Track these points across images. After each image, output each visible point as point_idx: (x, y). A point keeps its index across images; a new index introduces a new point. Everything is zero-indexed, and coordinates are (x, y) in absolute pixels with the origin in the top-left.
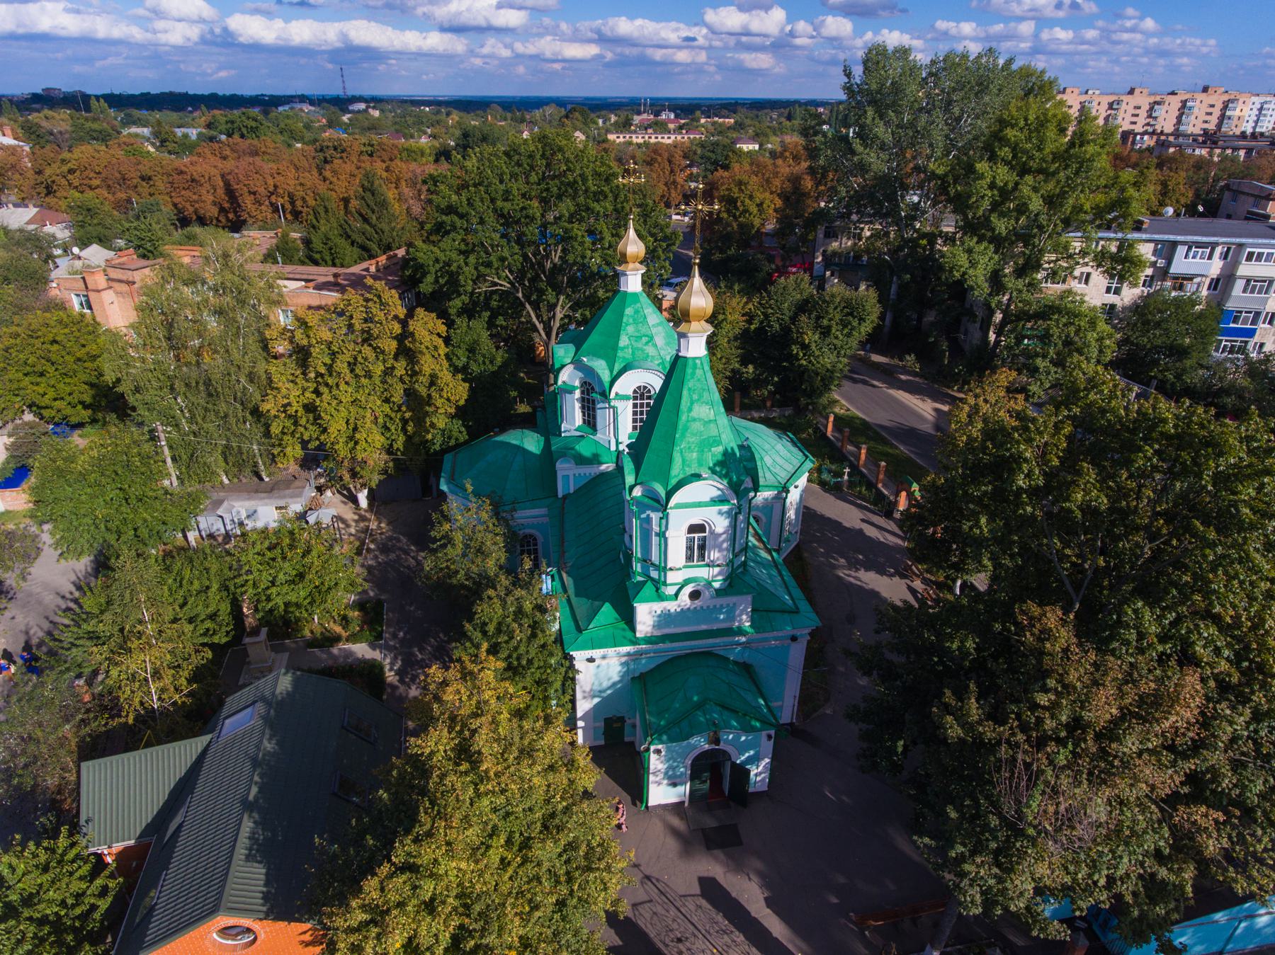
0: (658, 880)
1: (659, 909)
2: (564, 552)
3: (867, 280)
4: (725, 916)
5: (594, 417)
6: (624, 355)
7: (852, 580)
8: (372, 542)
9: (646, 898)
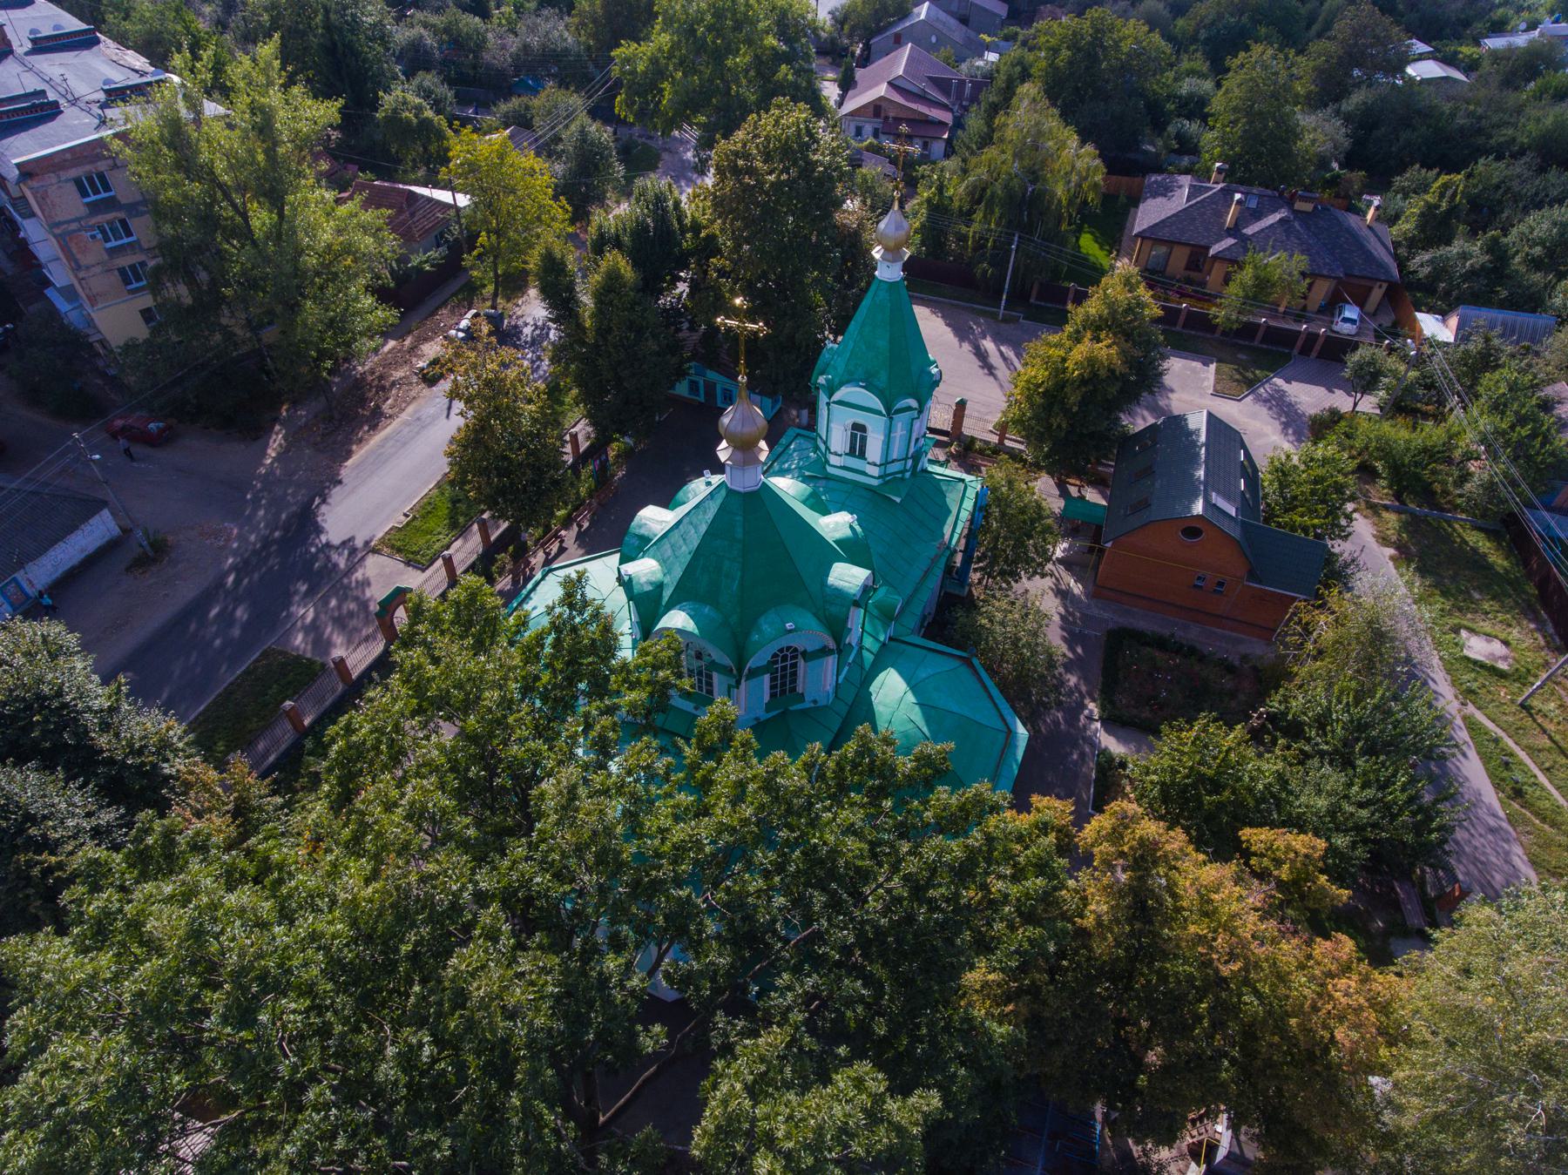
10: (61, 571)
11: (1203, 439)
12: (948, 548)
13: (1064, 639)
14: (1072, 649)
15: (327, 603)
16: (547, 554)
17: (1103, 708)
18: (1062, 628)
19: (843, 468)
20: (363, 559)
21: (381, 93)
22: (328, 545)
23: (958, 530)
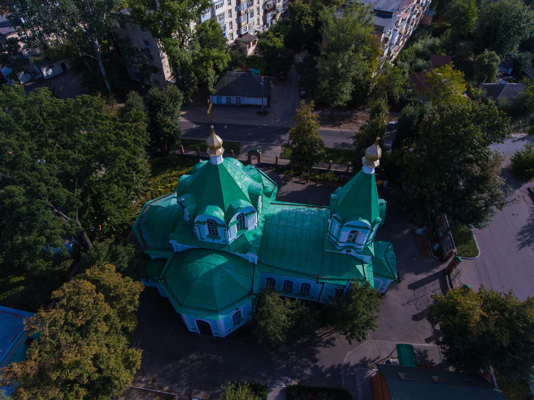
0: (409, 300)
1: (419, 303)
2: (306, 273)
3: (44, 66)
4: (421, 286)
5: (244, 224)
6: (245, 191)
7: (285, 194)
8: (161, 388)
9: (415, 305)
12: (318, 279)
13: (332, 367)
14: (327, 371)
16: (300, 181)
18: (339, 365)
20: (278, 145)
21: (486, 49)
22: (280, 137)
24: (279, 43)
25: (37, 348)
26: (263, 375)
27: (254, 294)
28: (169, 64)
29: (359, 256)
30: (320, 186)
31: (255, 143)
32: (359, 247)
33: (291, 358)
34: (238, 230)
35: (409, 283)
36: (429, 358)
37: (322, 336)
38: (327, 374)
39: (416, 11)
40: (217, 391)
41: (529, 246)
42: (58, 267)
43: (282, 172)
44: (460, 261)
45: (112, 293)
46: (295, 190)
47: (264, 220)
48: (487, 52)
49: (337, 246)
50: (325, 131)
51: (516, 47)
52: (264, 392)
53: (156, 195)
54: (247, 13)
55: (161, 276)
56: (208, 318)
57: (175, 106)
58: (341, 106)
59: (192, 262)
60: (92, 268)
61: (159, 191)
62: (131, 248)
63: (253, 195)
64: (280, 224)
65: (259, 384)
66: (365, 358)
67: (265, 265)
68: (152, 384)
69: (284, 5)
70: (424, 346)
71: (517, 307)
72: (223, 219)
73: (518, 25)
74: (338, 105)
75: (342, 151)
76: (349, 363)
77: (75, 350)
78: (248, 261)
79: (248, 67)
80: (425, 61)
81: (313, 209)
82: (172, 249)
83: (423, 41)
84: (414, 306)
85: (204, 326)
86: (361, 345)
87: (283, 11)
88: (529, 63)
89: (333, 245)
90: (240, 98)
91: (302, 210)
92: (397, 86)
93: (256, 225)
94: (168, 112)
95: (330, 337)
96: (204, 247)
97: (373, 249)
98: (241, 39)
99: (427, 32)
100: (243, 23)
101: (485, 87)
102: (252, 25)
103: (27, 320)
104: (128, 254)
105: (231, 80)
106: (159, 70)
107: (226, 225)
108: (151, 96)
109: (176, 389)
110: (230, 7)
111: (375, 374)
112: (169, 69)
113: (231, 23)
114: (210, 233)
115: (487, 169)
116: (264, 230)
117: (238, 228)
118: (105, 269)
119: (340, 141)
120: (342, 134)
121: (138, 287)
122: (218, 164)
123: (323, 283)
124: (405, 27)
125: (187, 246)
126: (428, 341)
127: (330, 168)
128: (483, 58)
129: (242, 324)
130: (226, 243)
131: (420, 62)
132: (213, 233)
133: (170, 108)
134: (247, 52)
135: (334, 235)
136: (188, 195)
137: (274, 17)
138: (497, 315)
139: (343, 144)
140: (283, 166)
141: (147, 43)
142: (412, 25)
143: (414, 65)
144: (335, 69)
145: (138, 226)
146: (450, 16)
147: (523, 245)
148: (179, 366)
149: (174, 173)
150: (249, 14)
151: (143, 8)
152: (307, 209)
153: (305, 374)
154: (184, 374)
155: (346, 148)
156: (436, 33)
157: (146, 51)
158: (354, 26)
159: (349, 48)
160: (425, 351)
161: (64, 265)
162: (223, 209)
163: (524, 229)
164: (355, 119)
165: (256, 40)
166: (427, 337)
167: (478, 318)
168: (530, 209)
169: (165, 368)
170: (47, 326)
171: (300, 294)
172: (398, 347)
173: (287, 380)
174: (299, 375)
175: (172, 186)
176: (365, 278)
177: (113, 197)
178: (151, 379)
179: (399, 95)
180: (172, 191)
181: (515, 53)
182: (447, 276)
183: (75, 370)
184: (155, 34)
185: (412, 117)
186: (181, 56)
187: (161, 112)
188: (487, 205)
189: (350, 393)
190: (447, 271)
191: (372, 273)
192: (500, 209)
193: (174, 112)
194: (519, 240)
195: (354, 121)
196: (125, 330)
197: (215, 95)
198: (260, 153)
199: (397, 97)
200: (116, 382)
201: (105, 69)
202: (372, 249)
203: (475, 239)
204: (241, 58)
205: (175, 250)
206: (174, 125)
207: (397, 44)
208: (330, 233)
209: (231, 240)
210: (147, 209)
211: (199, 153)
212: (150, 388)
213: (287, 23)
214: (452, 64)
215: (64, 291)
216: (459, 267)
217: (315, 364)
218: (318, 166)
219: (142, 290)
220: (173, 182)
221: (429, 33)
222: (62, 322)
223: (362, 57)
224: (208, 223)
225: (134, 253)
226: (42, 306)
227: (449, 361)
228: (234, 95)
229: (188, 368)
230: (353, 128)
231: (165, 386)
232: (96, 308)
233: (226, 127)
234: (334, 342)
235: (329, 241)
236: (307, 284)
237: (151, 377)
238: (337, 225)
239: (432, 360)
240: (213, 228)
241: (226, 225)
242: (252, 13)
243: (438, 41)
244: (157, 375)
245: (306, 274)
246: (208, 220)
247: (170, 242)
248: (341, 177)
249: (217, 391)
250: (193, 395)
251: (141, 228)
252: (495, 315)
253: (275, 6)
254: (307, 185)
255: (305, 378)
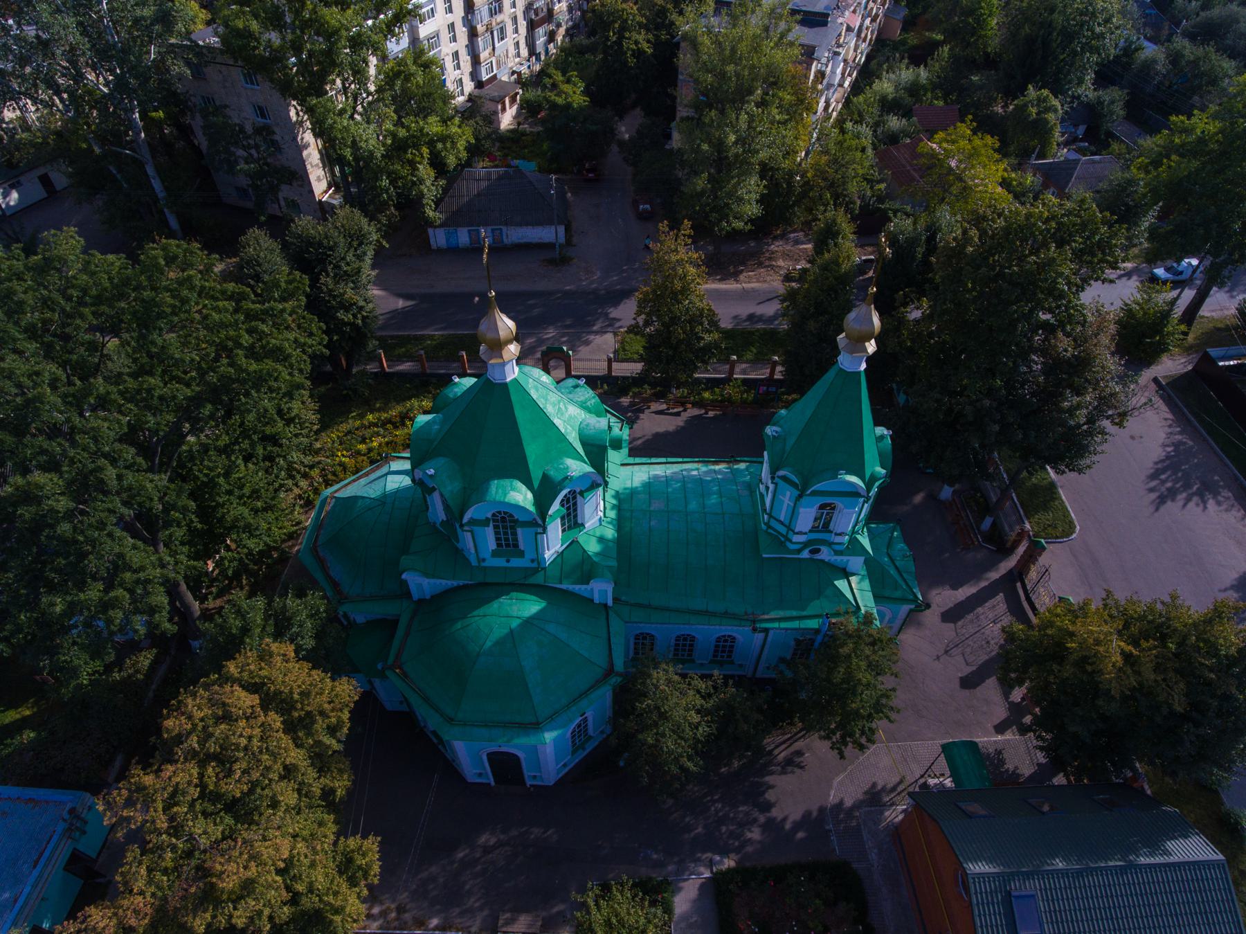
1: (968, 650)
5: (575, 516)
6: (573, 438)
7: (639, 442)
10: (525, 240)
11: (1143, 860)
12: (754, 622)
13: (807, 815)
14: (797, 826)
15: (563, 337)
16: (668, 409)
17: (729, 870)
18: (822, 810)
19: (762, 496)
20: (606, 332)
22: (607, 314)
23: (784, 625)
24: (575, 94)
25: (140, 863)
26: (655, 856)
27: (618, 674)
28: (322, 159)
29: (839, 560)
30: (715, 417)
31: (551, 333)
32: (838, 539)
33: (713, 809)
34: (563, 531)
35: (943, 610)
36: (1010, 766)
37: (773, 750)
38: (796, 832)
39: (872, 9)
40: (555, 910)
41: (1173, 500)
42: (119, 671)
43: (624, 392)
44: (1044, 549)
45: (296, 709)
46: (661, 430)
47: (614, 502)
48: (1032, 92)
49: (788, 544)
50: (726, 291)
51: (1090, 77)
52: (665, 895)
53: (334, 474)
54: (489, 29)
55: (391, 660)
56: (518, 744)
57: (360, 258)
58: (741, 230)
59: (464, 617)
60: (241, 659)
61: (341, 464)
62: (315, 599)
63: (592, 445)
64: (652, 509)
65: (651, 879)
66: (874, 785)
67: (631, 605)
68: (397, 919)
69: (570, 9)
70: (995, 742)
71: (1195, 625)
72: (532, 509)
73: (1088, 30)
74: (733, 229)
75: (751, 333)
76: (841, 803)
77: (241, 854)
78: (592, 601)
79: (505, 156)
80: (904, 120)
81: (717, 467)
82: (407, 594)
83: (892, 76)
84: (960, 659)
85: (506, 766)
86: (861, 758)
87: (570, 23)
88: (1119, 110)
89: (780, 542)
90: (501, 229)
91: (695, 473)
92: (854, 177)
93: (601, 514)
94: (345, 272)
95: (792, 749)
96: (489, 580)
97: (867, 540)
98: (477, 92)
99: (897, 55)
100: (484, 55)
101: (1037, 169)
102: (503, 59)
103: (104, 798)
104: (311, 616)
105: (475, 188)
106: (299, 176)
107: (538, 523)
108: (300, 236)
109: (459, 920)
110: (450, 18)
111: (901, 817)
112: (321, 172)
113: (456, 55)
114: (499, 545)
115: (1086, 341)
116: (620, 524)
117: (562, 525)
118: (271, 656)
119: (744, 310)
120: (745, 295)
121: (347, 689)
122: (508, 380)
123: (766, 630)
124: (852, 45)
125: (444, 582)
126: (1000, 728)
127: (731, 372)
128: (1025, 105)
129: (590, 747)
130: (539, 563)
131: (894, 123)
132: (508, 545)
133: (348, 264)
134: (499, 123)
135: (782, 519)
136: (441, 461)
137: (551, 37)
138: (1155, 647)
139: (751, 317)
140: (624, 378)
141: (261, 111)
142: (864, 40)
143: (879, 131)
144: (720, 146)
145: (314, 549)
146: (941, 16)
147: (1162, 500)
148: (456, 865)
149: (370, 417)
150: (495, 33)
151: (255, 26)
152: (704, 468)
153: (750, 839)
154: (471, 882)
155: (760, 326)
156: (918, 57)
157: (264, 131)
158: (756, 49)
159: (747, 98)
160: (999, 752)
161: (133, 665)
162: (529, 485)
163: (1160, 466)
164: (770, 259)
165: (518, 93)
166: (997, 722)
167: (1117, 658)
168: (1164, 423)
169: (424, 875)
170: (160, 806)
171: (711, 662)
172: (946, 748)
173: (711, 860)
174: (737, 844)
175: (370, 450)
176: (858, 607)
177: (241, 487)
178: (393, 906)
179: (859, 198)
180: (372, 462)
181: (1087, 90)
182: (1019, 585)
183: (246, 903)
184: (287, 90)
185: (912, 242)
186: (358, 139)
187: (328, 275)
188: (1091, 420)
189: (855, 866)
190: (1018, 574)
191: (870, 594)
192: (1120, 425)
193: (359, 271)
194: (1151, 490)
195: (767, 263)
196: (328, 793)
197: (441, 226)
198: (571, 352)
199: (854, 203)
200: (338, 918)
201: (163, 182)
202: (865, 541)
203: (1064, 498)
204: (489, 136)
205: (416, 595)
206: (362, 303)
207: (841, 85)
208: (770, 516)
209: (549, 555)
210: (327, 508)
211: (423, 366)
212: (395, 929)
213: (582, 51)
214: (971, 121)
215: (190, 717)
216: (1043, 560)
217: (768, 815)
218: (707, 371)
219: (356, 698)
220: (370, 439)
221: (902, 58)
222: (195, 792)
223: (778, 117)
224: (494, 521)
225: (324, 611)
226: (134, 761)
227: (1056, 762)
228: (486, 224)
229: (479, 867)
230: (768, 278)
231: (430, 918)
232: (267, 748)
233: (477, 299)
234: (801, 759)
235: (770, 534)
236: (729, 636)
237: (394, 901)
238: (787, 496)
239: (1016, 768)
240: (506, 533)
241: (540, 522)
242: (502, 28)
243: (923, 74)
244: (407, 894)
245: (726, 615)
246: (494, 515)
247: (404, 576)
248: (761, 392)
249: (555, 910)
250: (502, 926)
251: (321, 554)
252: (1150, 649)
253: (550, 12)
254: (685, 416)
255: (749, 849)
